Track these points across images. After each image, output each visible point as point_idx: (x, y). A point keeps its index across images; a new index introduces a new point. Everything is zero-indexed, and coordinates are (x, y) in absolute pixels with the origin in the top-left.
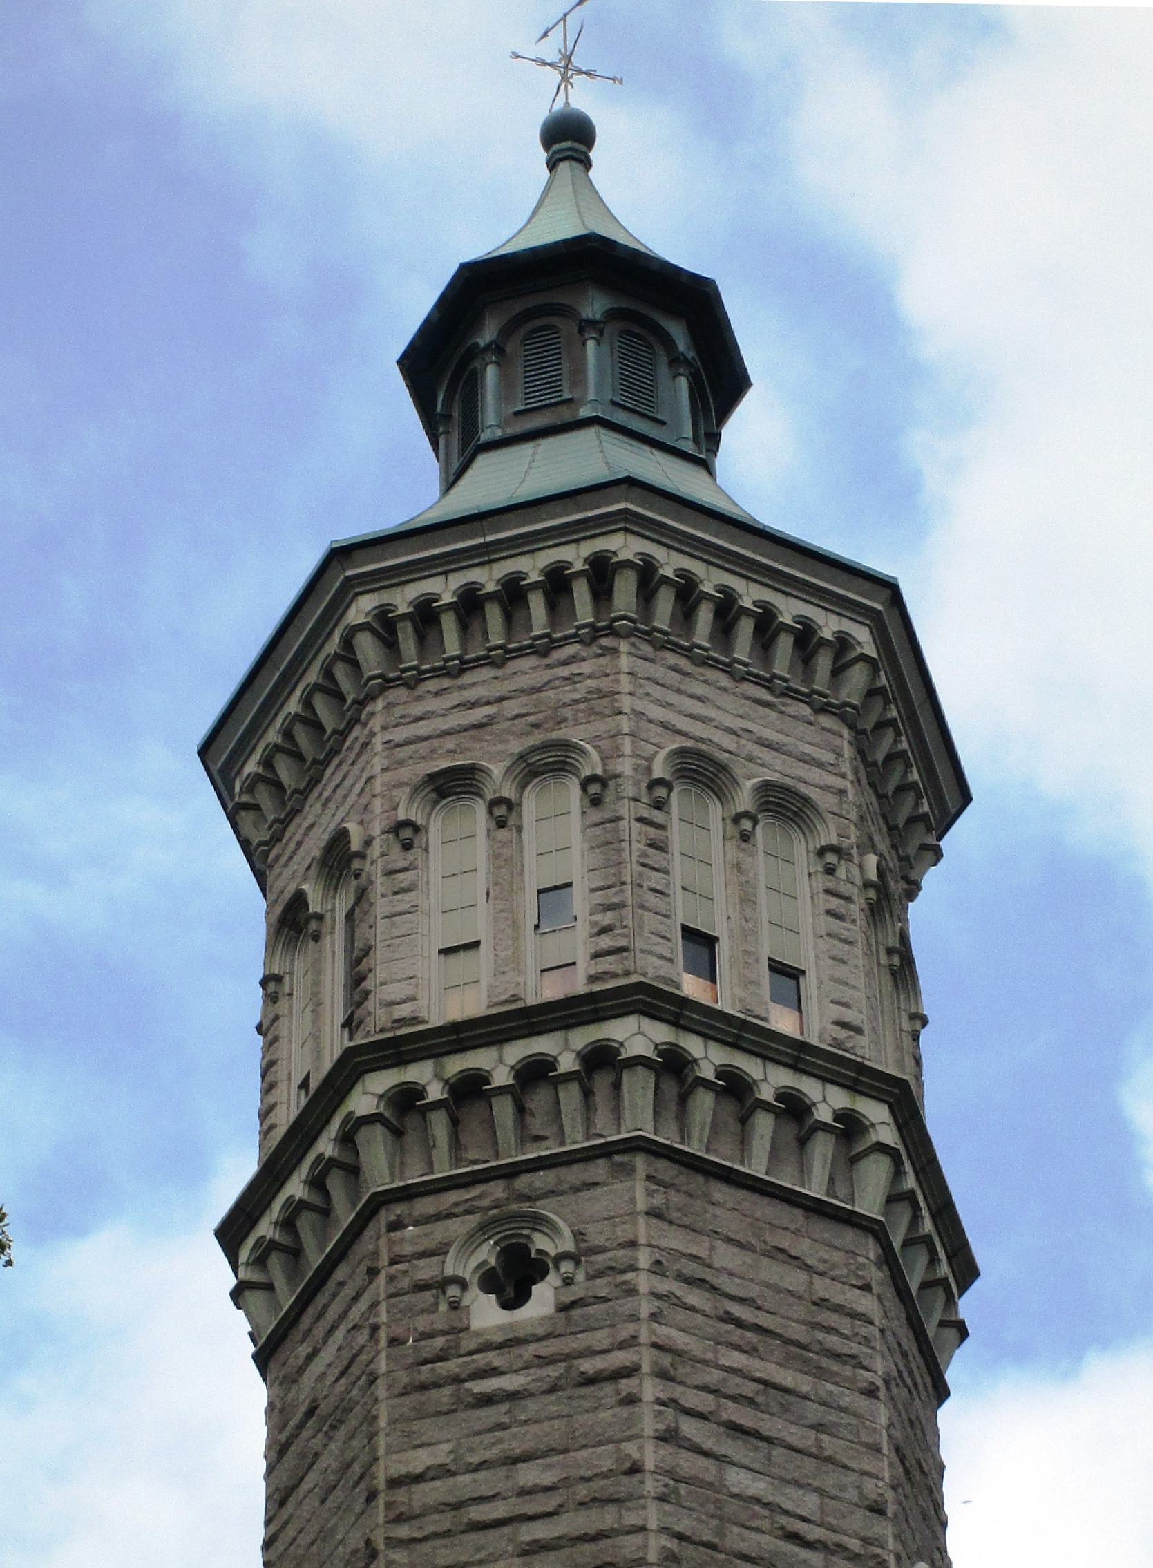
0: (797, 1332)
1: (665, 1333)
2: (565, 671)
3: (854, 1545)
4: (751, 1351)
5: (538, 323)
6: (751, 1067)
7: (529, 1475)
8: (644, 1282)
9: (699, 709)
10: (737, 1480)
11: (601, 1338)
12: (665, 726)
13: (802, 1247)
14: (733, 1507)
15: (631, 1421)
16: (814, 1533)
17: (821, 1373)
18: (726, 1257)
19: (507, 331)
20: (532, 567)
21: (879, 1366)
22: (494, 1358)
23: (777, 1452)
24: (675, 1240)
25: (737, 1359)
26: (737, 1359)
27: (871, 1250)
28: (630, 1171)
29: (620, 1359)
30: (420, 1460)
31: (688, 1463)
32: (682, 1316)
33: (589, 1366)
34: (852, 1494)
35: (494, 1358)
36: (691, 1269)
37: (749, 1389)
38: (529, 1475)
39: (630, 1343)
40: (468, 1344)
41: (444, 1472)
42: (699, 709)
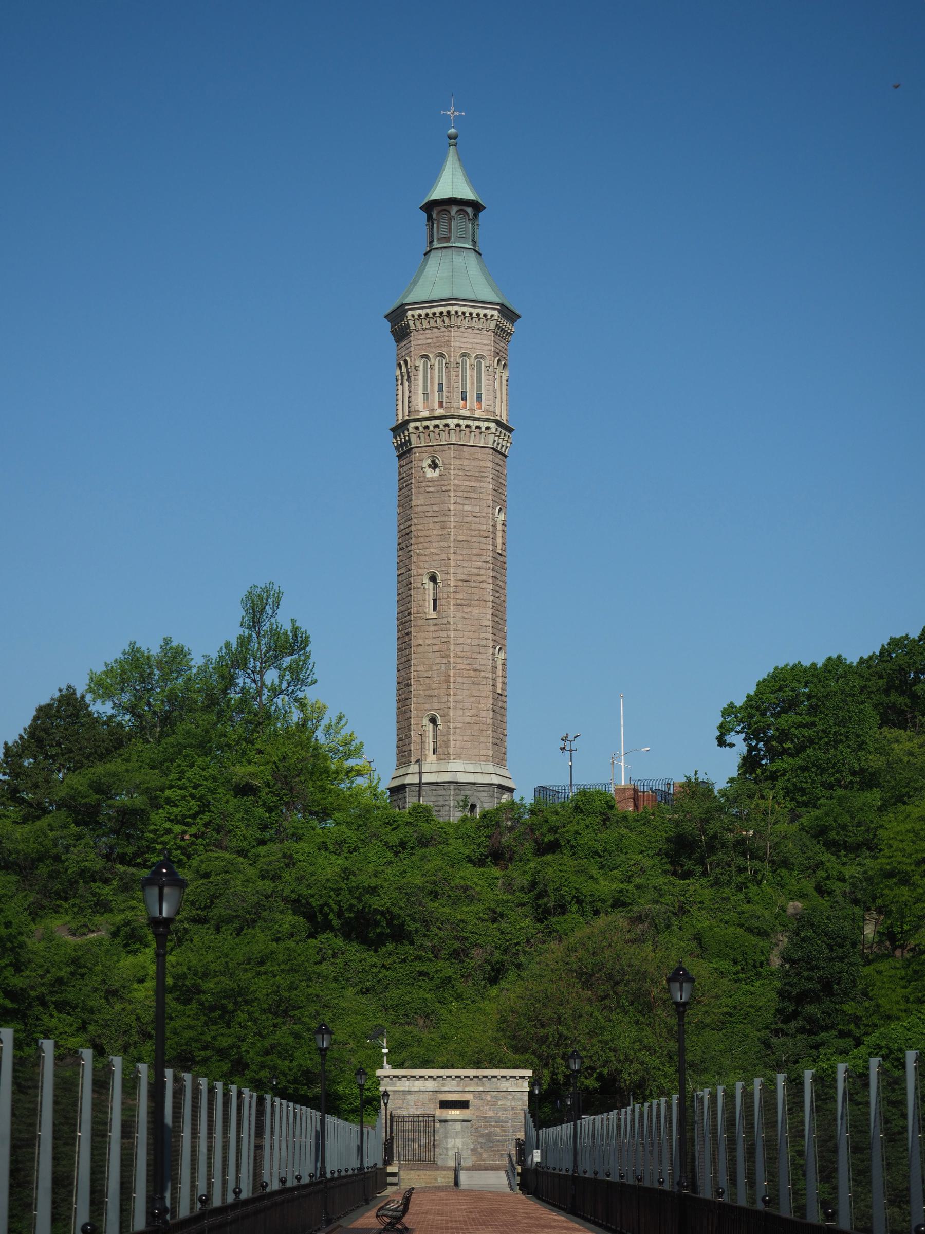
0: (477, 474)
1: (456, 482)
2: (442, 334)
3: (484, 515)
4: (469, 481)
5: (444, 207)
6: (470, 423)
7: (435, 508)
8: (452, 472)
9: (466, 340)
10: (467, 508)
11: (446, 482)
12: (460, 347)
13: (480, 456)
14: (465, 514)
15: (450, 500)
16: (478, 514)
17: (481, 481)
18: (466, 462)
19: (438, 214)
20: (437, 310)
21: (491, 477)
22: (430, 484)
23: (473, 500)
24: (458, 462)
25: (467, 483)
26: (467, 483)
27: (491, 451)
28: (450, 448)
29: (448, 488)
30: (419, 502)
31: (460, 507)
32: (457, 477)
33: (444, 488)
34: (485, 505)
35: (430, 484)
36: (460, 467)
37: (468, 489)
38: (435, 508)
39: (449, 485)
40: (426, 480)
41: (422, 505)
42: (466, 340)
